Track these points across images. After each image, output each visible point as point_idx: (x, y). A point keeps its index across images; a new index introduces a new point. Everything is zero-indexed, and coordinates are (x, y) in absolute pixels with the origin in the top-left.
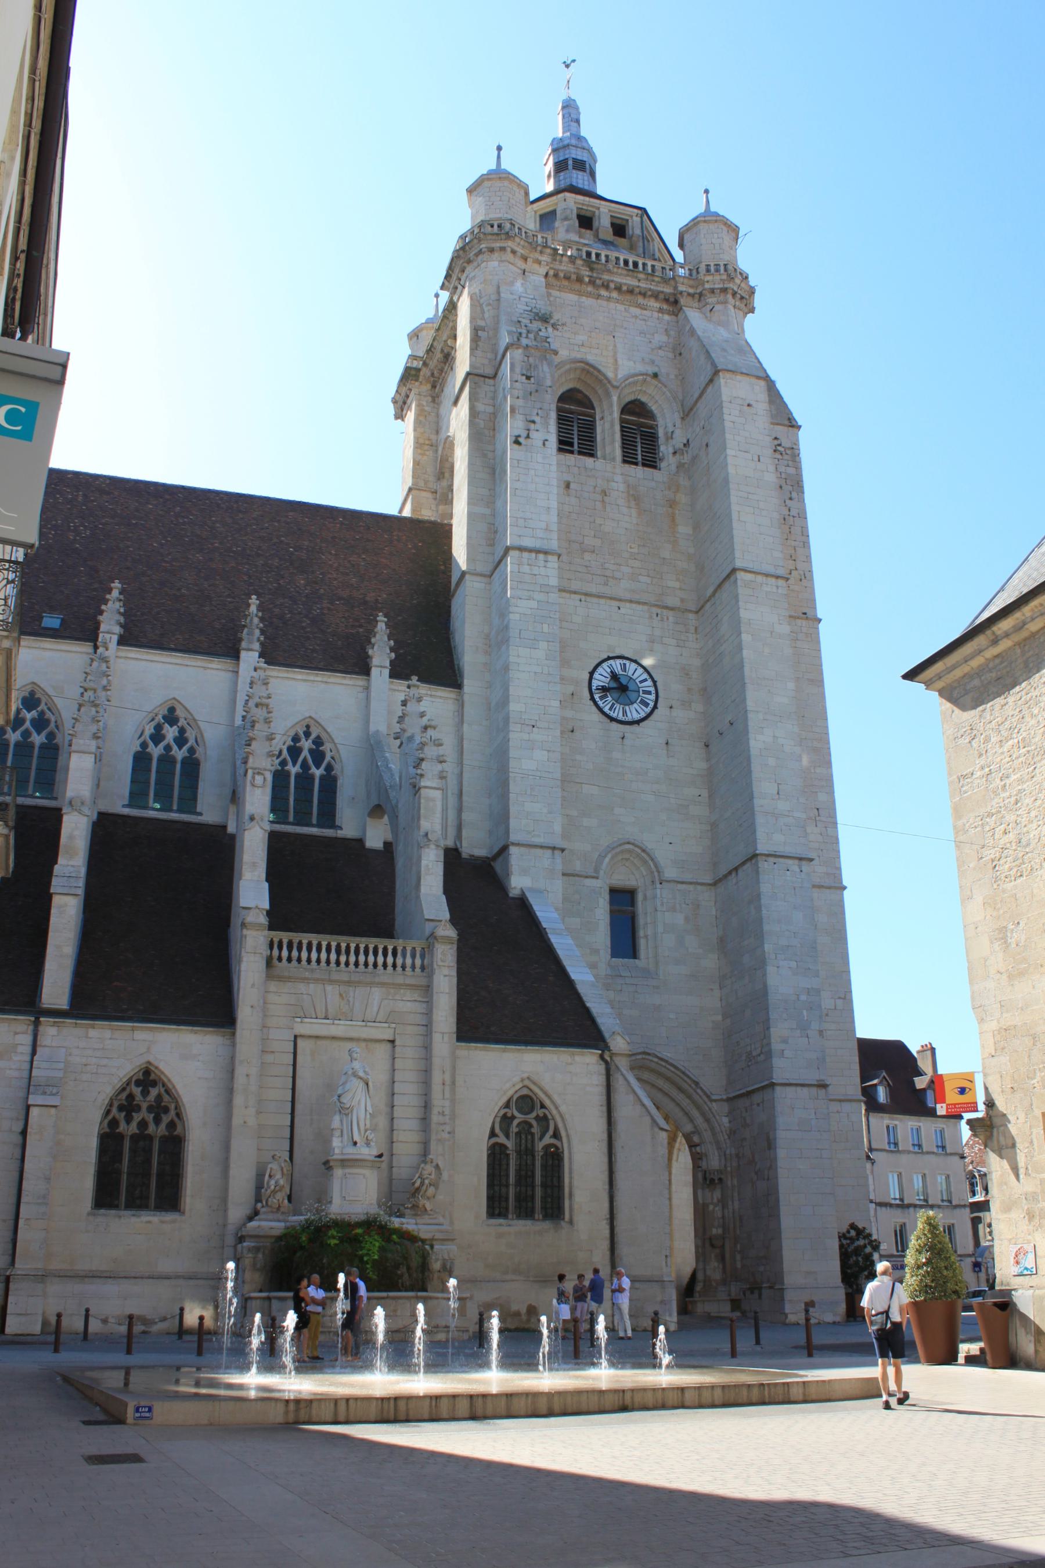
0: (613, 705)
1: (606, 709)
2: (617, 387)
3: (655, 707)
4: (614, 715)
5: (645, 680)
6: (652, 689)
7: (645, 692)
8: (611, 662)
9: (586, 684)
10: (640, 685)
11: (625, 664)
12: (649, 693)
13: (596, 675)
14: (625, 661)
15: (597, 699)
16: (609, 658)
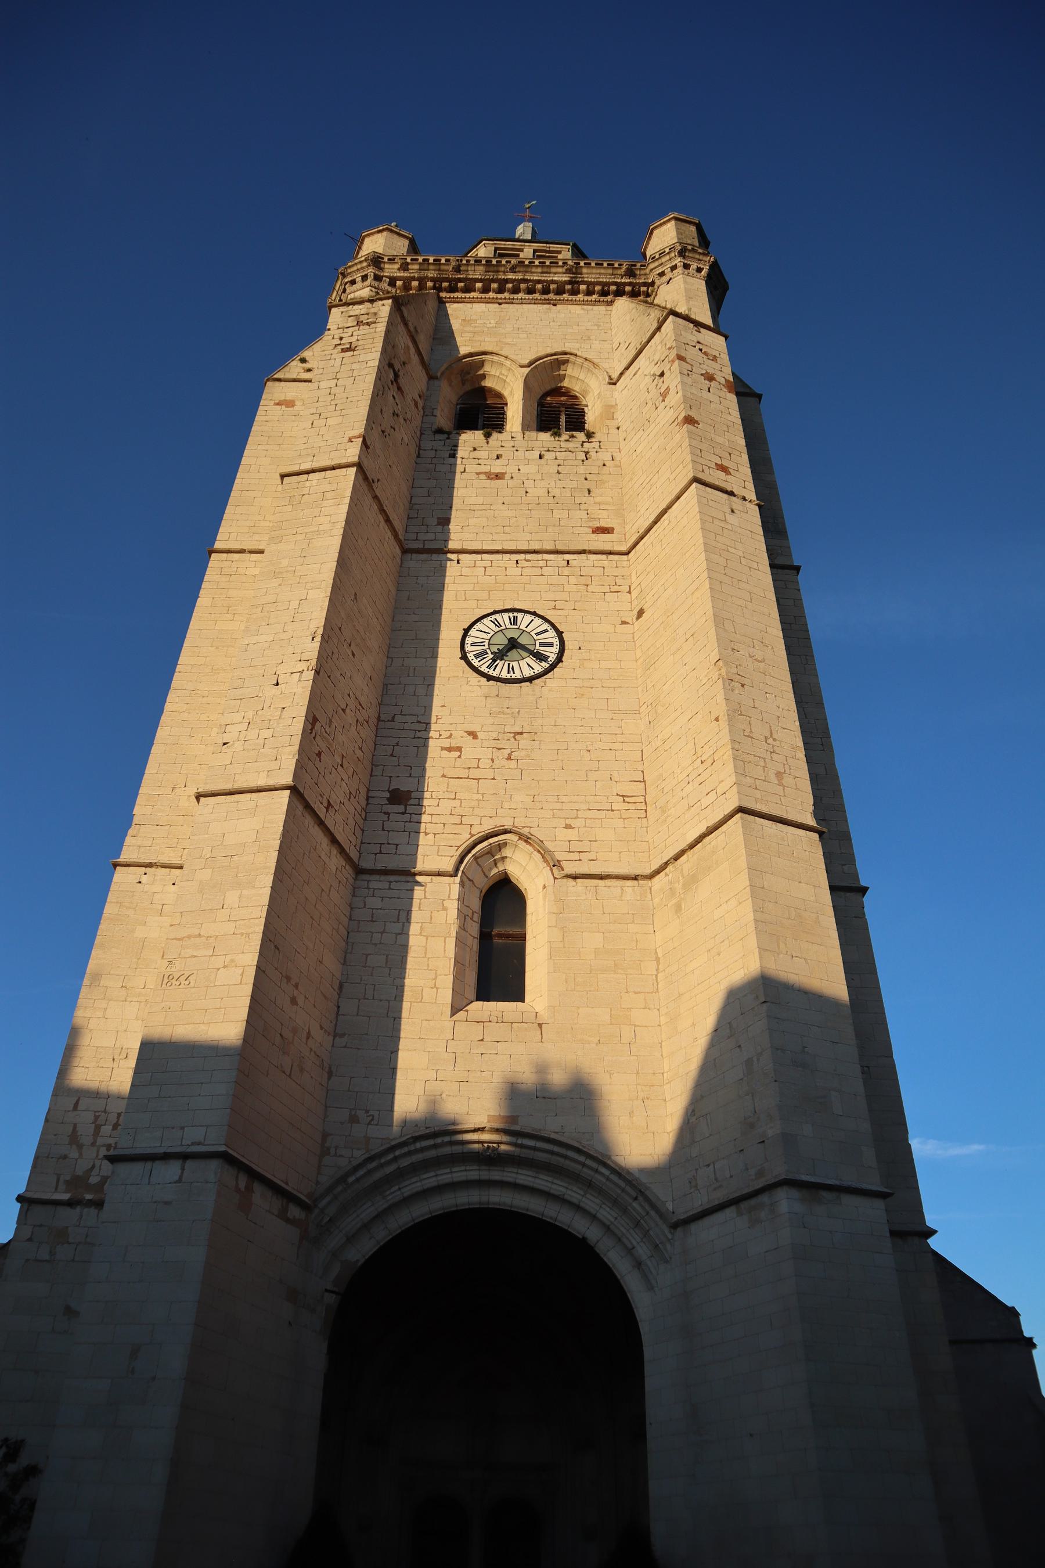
1: (484, 669)
3: (559, 659)
5: (546, 631)
8: (498, 616)
11: (515, 618)
12: (551, 645)
13: (473, 632)
14: (515, 614)
16: (495, 612)
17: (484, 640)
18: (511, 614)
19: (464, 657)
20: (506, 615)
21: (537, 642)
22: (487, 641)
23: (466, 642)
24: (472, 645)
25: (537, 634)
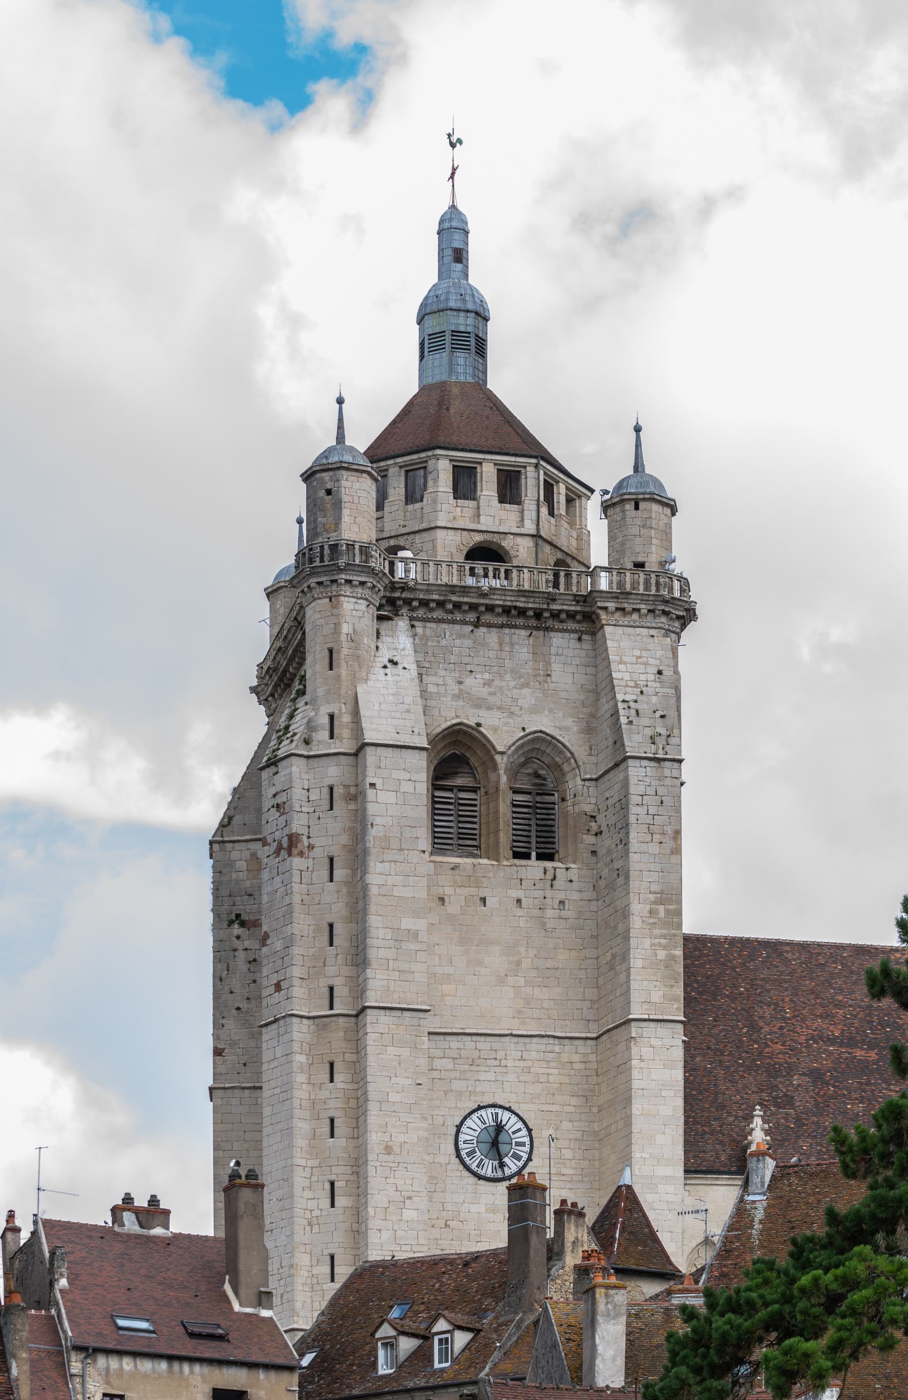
0: (482, 1160)
1: (474, 1167)
2: (502, 753)
4: (482, 1173)
5: (519, 1130)
6: (527, 1140)
7: (518, 1144)
8: (482, 1112)
9: (451, 1140)
10: (513, 1136)
11: (497, 1114)
12: (523, 1144)
13: (464, 1129)
14: (497, 1110)
15: (464, 1156)
16: (480, 1108)
17: (473, 1138)
18: (493, 1110)
19: (458, 1156)
20: (490, 1110)
21: (513, 1141)
22: (476, 1139)
23: (460, 1139)
24: (465, 1142)
25: (514, 1133)
